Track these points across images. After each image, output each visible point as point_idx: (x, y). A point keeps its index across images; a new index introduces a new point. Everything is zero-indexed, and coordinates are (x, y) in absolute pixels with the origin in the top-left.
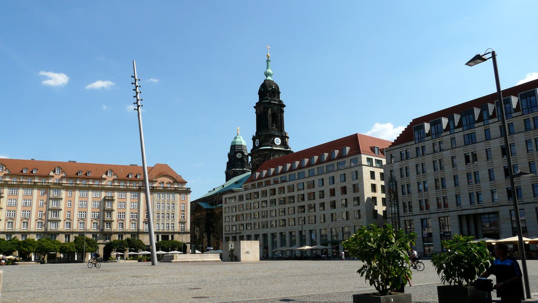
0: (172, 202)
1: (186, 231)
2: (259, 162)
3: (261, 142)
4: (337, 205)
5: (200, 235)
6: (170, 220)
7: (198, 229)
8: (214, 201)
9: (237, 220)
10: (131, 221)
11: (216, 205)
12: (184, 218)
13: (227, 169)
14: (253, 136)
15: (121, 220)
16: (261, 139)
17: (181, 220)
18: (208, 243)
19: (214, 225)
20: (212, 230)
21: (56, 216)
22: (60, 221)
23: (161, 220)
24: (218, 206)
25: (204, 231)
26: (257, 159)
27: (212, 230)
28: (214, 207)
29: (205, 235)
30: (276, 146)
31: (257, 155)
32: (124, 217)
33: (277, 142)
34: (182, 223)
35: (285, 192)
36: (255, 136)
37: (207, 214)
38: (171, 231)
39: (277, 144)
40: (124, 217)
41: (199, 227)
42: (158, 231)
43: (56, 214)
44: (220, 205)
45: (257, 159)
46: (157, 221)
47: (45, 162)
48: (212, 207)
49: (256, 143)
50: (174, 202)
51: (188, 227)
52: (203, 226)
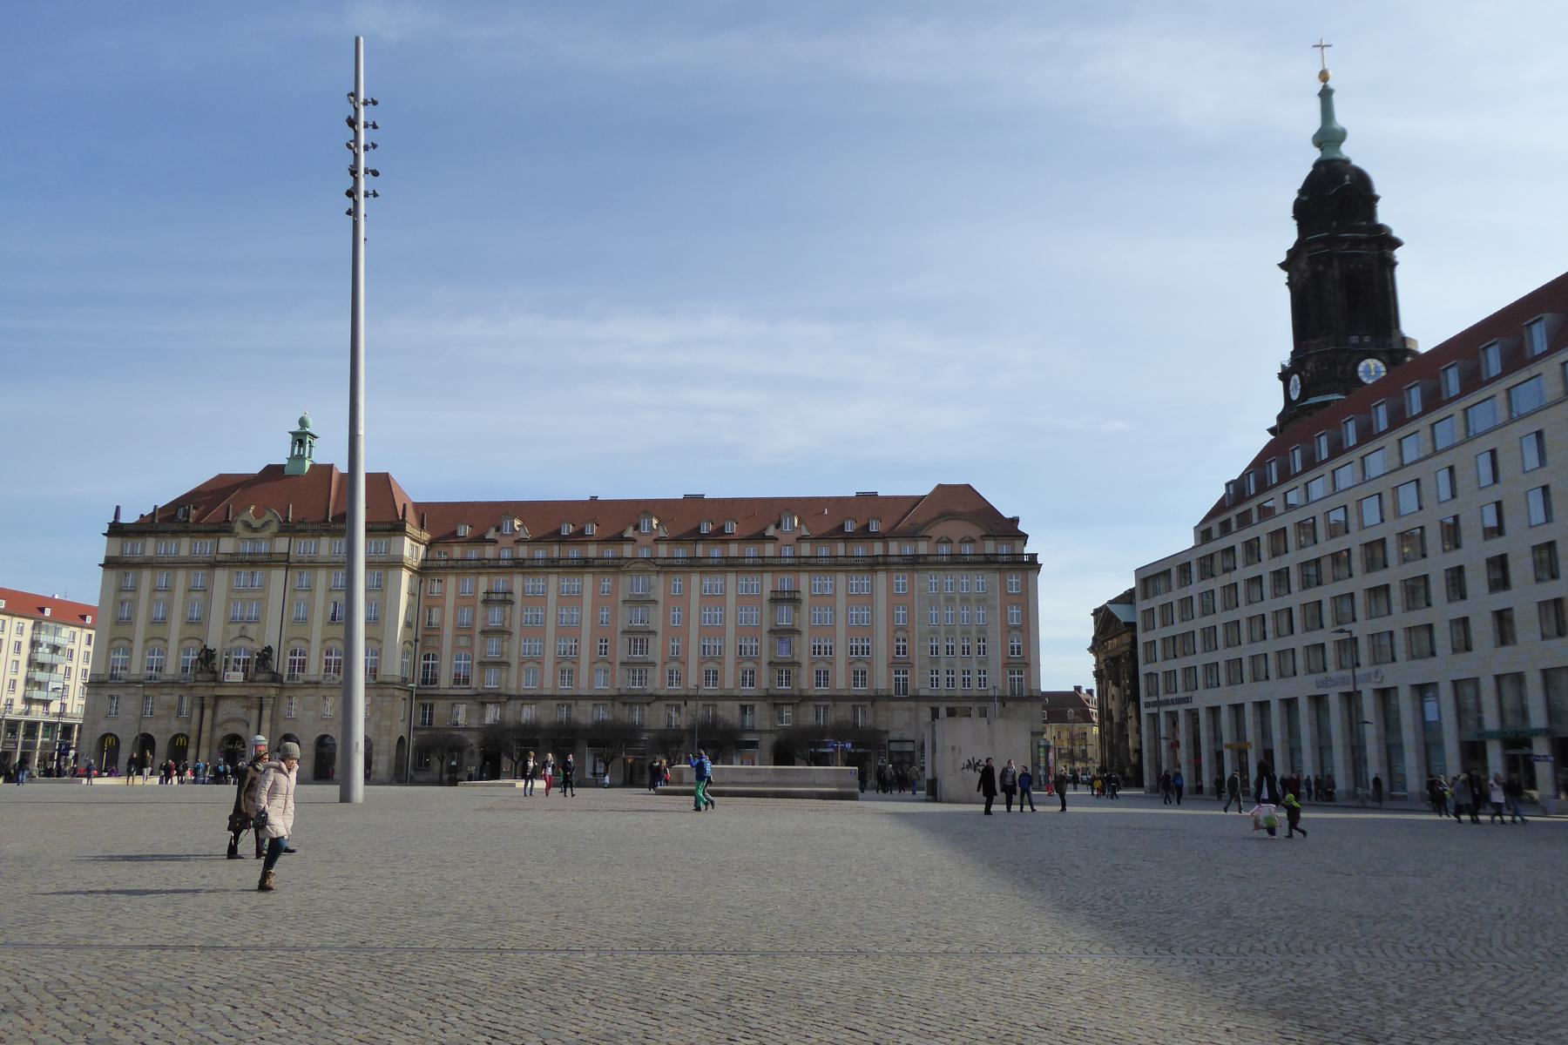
10: (850, 663)
17: (1009, 657)
21: (642, 653)
22: (653, 664)
32: (831, 653)
40: (831, 653)
43: (641, 647)
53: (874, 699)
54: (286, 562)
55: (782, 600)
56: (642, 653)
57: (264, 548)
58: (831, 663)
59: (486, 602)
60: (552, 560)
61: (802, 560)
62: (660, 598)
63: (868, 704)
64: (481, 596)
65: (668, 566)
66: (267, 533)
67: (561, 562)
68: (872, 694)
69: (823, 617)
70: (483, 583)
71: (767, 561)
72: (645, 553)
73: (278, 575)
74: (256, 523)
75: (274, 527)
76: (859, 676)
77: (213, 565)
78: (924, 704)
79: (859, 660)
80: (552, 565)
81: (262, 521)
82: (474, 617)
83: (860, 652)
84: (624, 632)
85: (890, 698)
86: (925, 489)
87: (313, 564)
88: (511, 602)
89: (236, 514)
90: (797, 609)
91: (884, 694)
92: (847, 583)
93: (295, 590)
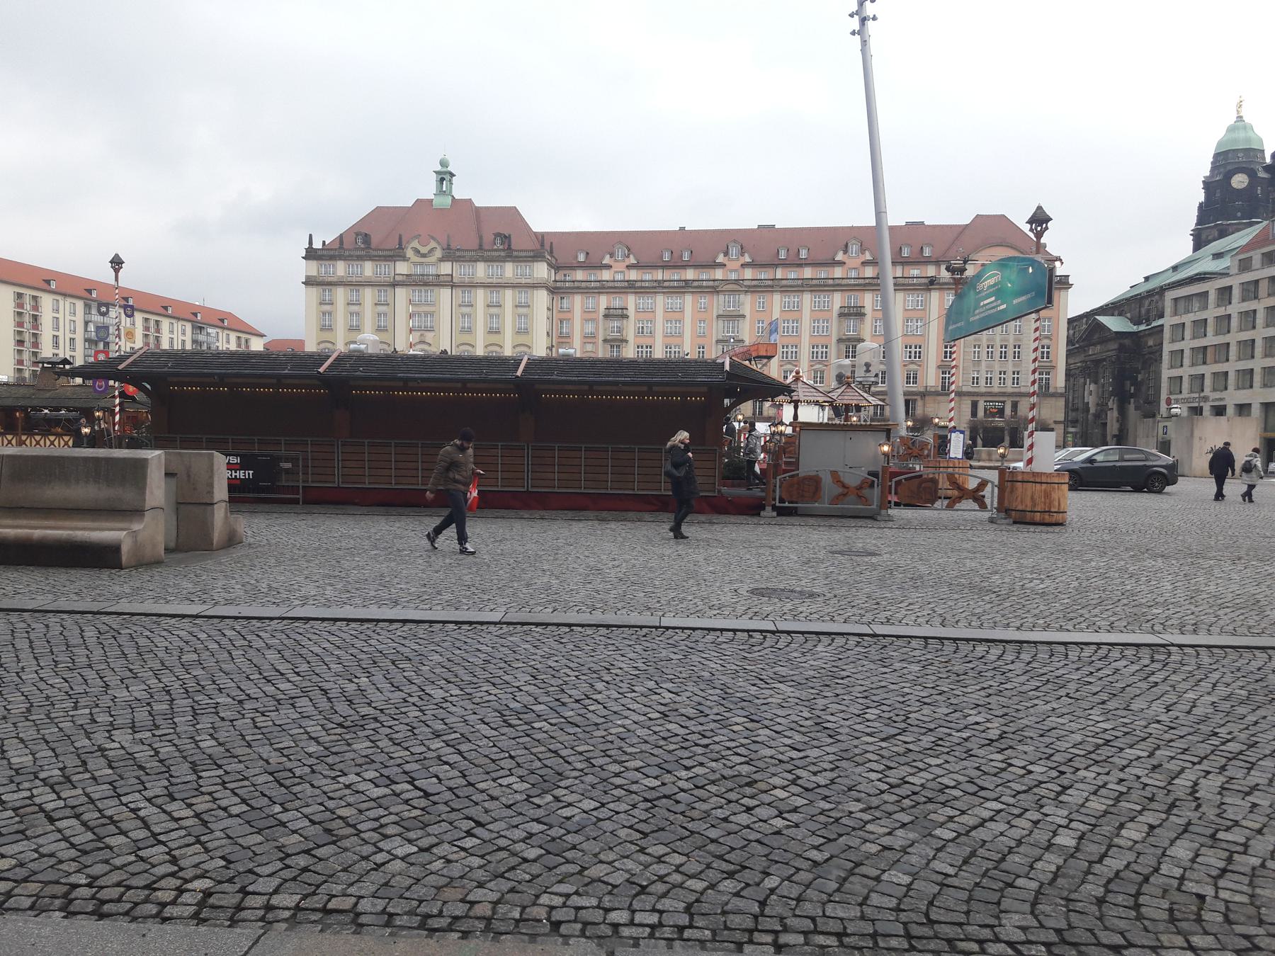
1: (1051, 390)
5: (1098, 404)
6: (1010, 363)
7: (1093, 387)
8: (1143, 311)
9: (1208, 361)
11: (1148, 322)
12: (1048, 358)
13: (1197, 224)
18: (1121, 425)
19: (1140, 377)
20: (1132, 391)
23: (983, 364)
24: (1154, 324)
25: (1112, 393)
27: (1132, 391)
28: (1143, 327)
29: (1112, 403)
37: (1122, 348)
38: (1010, 390)
41: (1096, 383)
42: (976, 390)
44: (1160, 322)
46: (974, 366)
47: (706, 231)
48: (1135, 328)
51: (1059, 381)
52: (1107, 380)
53: (924, 395)
54: (451, 284)
55: (849, 315)
57: (432, 271)
59: (606, 316)
60: (659, 281)
61: (867, 281)
62: (747, 313)
63: (918, 398)
64: (602, 311)
65: (755, 286)
66: (433, 259)
67: (666, 284)
70: (604, 301)
71: (837, 282)
72: (733, 276)
73: (445, 293)
74: (424, 250)
75: (438, 253)
77: (394, 285)
78: (966, 398)
79: (912, 363)
80: (658, 287)
81: (429, 248)
82: (597, 329)
84: (718, 341)
85: (937, 394)
86: (966, 220)
87: (473, 286)
88: (627, 317)
89: (408, 242)
90: (862, 321)
92: (905, 300)
93: (460, 306)
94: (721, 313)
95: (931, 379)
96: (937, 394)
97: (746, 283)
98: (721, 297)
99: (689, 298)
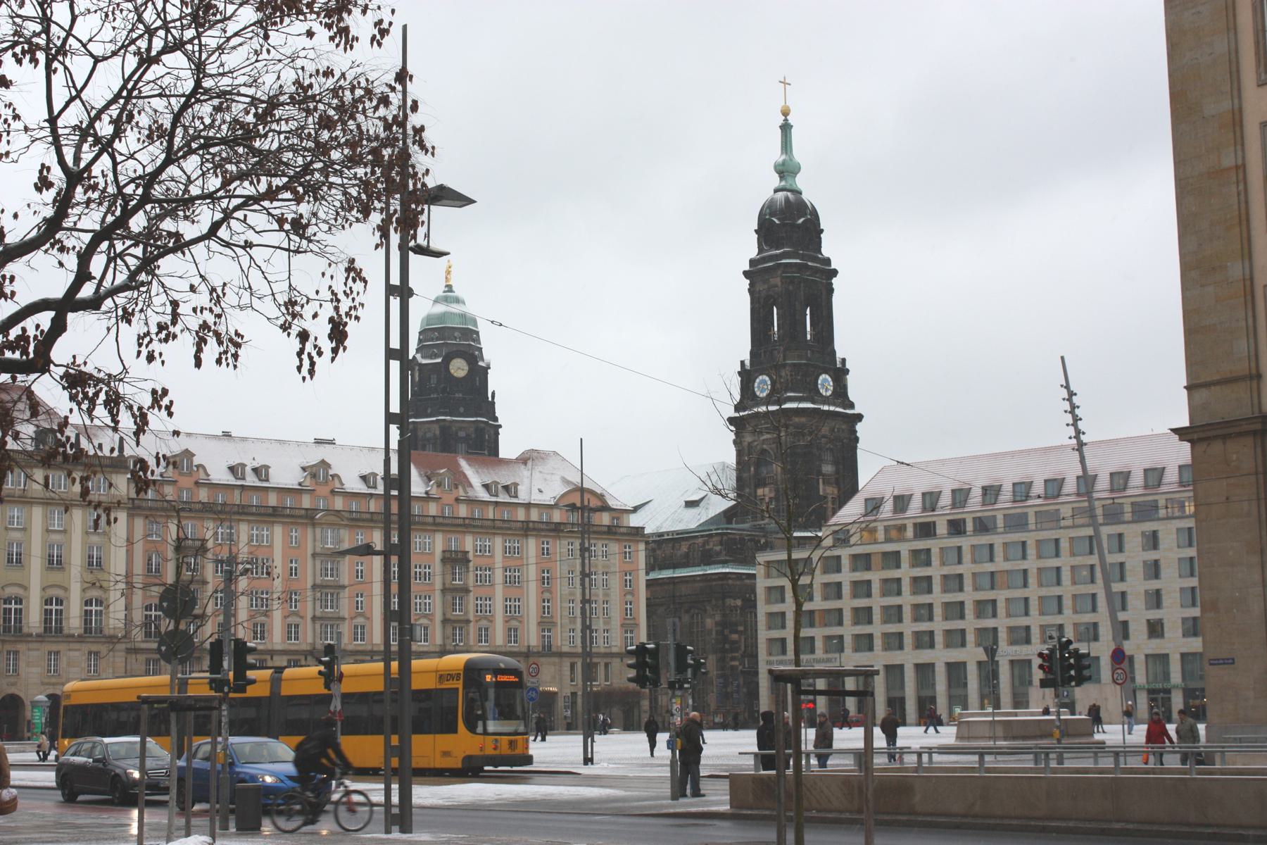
0: (603, 567)
2: (774, 446)
3: (778, 386)
4: (1166, 601)
14: (742, 363)
15: (486, 618)
16: (781, 377)
26: (766, 436)
30: (826, 401)
31: (766, 423)
33: (823, 385)
34: (629, 626)
35: (996, 559)
36: (747, 363)
39: (823, 391)
42: (573, 650)
45: (766, 436)
49: (756, 385)
50: (608, 567)
56: (332, 607)
58: (491, 621)
61: (467, 521)
68: (524, 650)
69: (483, 576)
76: (512, 633)
83: (513, 613)
91: (535, 650)
94: (318, 550)
95: (532, 637)
96: (539, 654)
97: (347, 515)
98: (318, 531)
99: (278, 530)
